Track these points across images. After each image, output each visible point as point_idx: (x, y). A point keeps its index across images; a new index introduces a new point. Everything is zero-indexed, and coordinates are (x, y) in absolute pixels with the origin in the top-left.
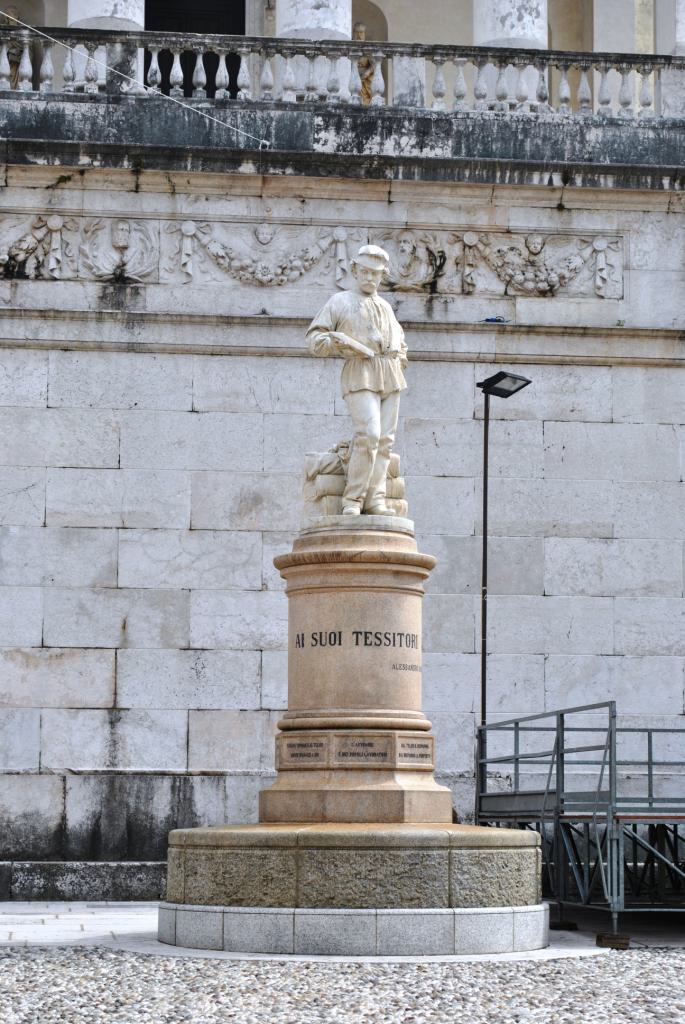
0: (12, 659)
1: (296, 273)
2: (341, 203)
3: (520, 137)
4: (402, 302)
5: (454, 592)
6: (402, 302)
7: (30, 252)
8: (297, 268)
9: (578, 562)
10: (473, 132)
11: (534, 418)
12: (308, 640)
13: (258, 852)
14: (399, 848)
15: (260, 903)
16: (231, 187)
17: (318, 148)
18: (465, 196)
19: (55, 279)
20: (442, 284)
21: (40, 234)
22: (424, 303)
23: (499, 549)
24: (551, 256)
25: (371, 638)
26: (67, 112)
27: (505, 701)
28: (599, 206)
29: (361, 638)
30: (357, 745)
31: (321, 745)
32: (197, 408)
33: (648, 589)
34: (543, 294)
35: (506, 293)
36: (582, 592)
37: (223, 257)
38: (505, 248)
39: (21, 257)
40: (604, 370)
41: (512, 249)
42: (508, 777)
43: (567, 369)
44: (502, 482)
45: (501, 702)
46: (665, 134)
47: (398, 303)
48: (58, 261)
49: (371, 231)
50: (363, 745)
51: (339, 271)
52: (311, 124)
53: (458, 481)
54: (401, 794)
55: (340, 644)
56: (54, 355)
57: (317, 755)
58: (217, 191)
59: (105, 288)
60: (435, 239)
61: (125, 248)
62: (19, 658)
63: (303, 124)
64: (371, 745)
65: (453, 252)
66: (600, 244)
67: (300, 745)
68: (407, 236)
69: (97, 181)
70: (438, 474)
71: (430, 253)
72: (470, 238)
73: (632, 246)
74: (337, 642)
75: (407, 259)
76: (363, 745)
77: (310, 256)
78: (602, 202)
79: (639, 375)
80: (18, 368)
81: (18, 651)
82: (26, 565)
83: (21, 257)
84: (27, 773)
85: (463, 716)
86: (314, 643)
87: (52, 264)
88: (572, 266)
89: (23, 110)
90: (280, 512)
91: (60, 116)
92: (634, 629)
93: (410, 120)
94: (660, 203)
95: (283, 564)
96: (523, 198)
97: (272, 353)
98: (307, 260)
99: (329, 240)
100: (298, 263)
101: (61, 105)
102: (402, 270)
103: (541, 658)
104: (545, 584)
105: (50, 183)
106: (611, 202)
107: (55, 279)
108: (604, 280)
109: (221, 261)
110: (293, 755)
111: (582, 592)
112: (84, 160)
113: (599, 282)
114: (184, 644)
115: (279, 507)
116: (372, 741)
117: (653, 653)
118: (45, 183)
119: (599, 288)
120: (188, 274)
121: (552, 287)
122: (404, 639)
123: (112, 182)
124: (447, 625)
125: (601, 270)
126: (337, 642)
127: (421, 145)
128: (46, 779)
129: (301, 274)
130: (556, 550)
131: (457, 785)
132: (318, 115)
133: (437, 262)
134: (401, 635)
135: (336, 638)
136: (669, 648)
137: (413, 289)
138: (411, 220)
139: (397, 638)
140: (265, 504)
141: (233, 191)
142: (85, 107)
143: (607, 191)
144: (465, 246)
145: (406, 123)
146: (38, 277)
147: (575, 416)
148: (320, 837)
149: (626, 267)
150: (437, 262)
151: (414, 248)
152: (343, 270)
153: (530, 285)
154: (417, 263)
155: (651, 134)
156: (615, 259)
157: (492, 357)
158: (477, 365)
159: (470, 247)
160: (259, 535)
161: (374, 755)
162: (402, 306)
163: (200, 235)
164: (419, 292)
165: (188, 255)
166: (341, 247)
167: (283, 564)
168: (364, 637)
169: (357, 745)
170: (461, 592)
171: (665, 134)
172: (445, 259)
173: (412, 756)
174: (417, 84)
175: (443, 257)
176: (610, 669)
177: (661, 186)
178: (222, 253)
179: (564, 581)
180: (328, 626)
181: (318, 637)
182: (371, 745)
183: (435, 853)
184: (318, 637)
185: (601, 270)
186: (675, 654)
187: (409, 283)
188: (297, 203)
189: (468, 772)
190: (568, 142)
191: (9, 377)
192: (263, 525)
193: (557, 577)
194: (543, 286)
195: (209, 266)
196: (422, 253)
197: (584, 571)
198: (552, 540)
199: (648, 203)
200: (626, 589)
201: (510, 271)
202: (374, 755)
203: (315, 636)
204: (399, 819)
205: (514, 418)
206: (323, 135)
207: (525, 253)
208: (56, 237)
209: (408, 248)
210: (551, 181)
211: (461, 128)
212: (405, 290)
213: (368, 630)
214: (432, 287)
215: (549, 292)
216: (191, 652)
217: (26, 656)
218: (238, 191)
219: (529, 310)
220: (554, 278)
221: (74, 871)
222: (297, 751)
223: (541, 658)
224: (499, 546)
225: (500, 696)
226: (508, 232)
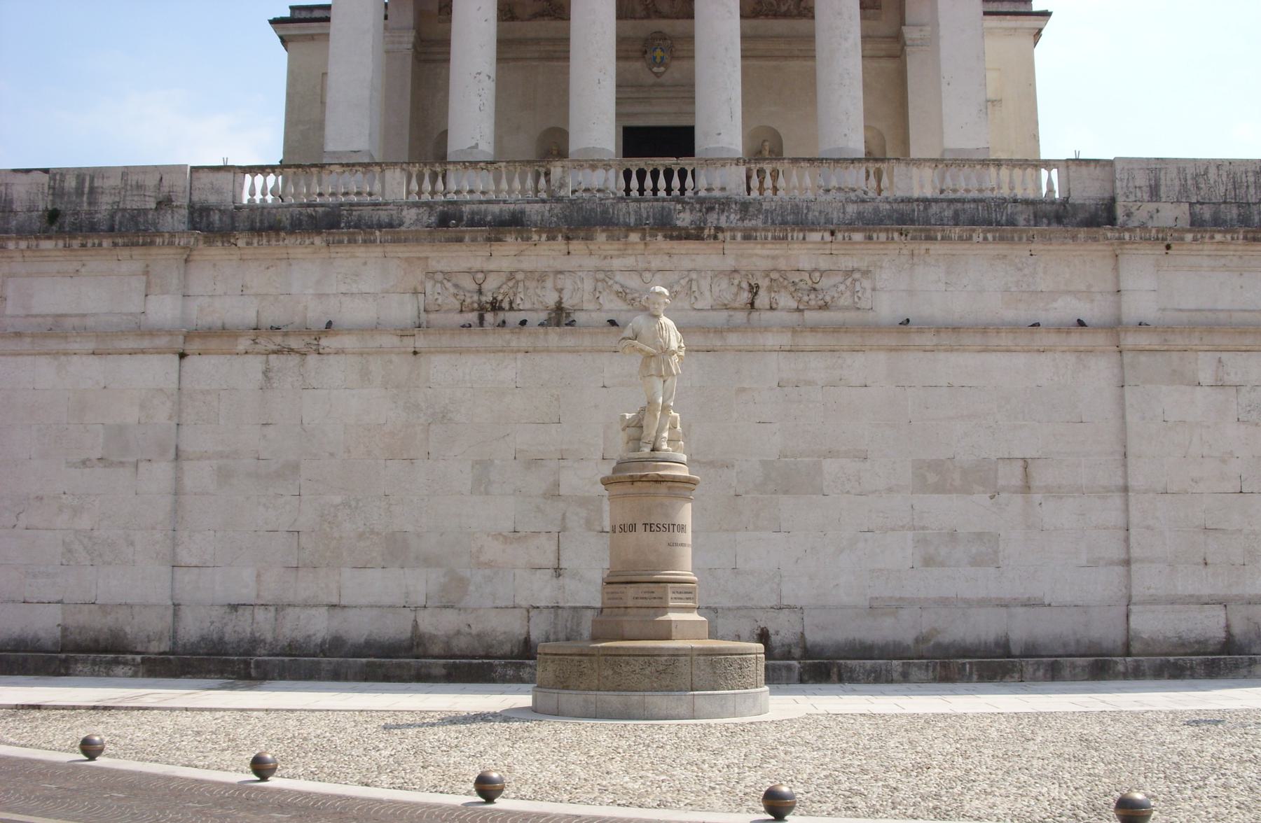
0: (497, 540)
2: (694, 257)
3: (805, 211)
7: (505, 294)
10: (775, 210)
11: (817, 385)
12: (618, 529)
13: (577, 658)
14: (659, 655)
15: (578, 688)
16: (625, 250)
17: (679, 223)
18: (771, 249)
19: (521, 310)
21: (511, 284)
24: (825, 283)
25: (654, 527)
26: (526, 210)
28: (855, 252)
29: (648, 527)
30: (645, 592)
32: (606, 384)
33: (890, 490)
34: (820, 308)
36: (848, 492)
38: (797, 280)
39: (500, 298)
40: (860, 354)
41: (801, 281)
43: (837, 354)
45: (797, 562)
46: (895, 206)
47: (730, 316)
48: (522, 299)
50: (649, 592)
52: (675, 209)
53: (768, 425)
54: (670, 622)
56: (520, 355)
58: (616, 253)
59: (549, 314)
61: (562, 289)
62: (501, 539)
63: (670, 209)
64: (653, 592)
65: (764, 283)
66: (857, 275)
69: (544, 250)
71: (750, 285)
72: (774, 275)
73: (877, 277)
75: (734, 289)
76: (649, 592)
78: (857, 249)
79: (882, 356)
80: (498, 365)
81: (500, 534)
82: (504, 482)
83: (500, 298)
84: (507, 608)
87: (518, 301)
88: (839, 290)
89: (501, 211)
91: (523, 212)
92: (881, 515)
93: (736, 203)
94: (895, 249)
95: (606, 482)
96: (808, 249)
99: (687, 279)
101: (523, 206)
102: (732, 296)
105: (516, 253)
106: (863, 249)
107: (521, 310)
108: (859, 298)
109: (620, 295)
111: (848, 492)
112: (535, 237)
113: (856, 300)
114: (599, 529)
117: (893, 530)
118: (513, 253)
119: (857, 303)
120: (600, 304)
121: (826, 303)
122: (676, 528)
123: (553, 250)
125: (858, 292)
127: (742, 219)
128: (517, 611)
130: (830, 466)
133: (754, 290)
134: (674, 525)
135: (633, 527)
136: (903, 527)
139: (671, 527)
141: (627, 252)
142: (537, 206)
143: (860, 243)
144: (772, 279)
145: (734, 206)
146: (511, 309)
148: (655, 649)
149: (874, 289)
150: (754, 290)
152: (695, 297)
153: (813, 303)
154: (742, 291)
155: (888, 207)
156: (867, 284)
157: (788, 348)
163: (607, 279)
165: (600, 292)
166: (694, 283)
167: (606, 482)
168: (649, 526)
169: (645, 592)
171: (895, 206)
173: (681, 599)
175: (758, 287)
176: (866, 540)
177: (893, 239)
178: (621, 290)
180: (629, 521)
181: (622, 527)
182: (653, 592)
183: (682, 658)
184: (622, 527)
185: (858, 292)
187: (737, 305)
188: (667, 258)
190: (835, 213)
191: (493, 370)
194: (821, 303)
195: (613, 297)
196: (745, 285)
197: (849, 480)
198: (829, 460)
199: (886, 249)
200: (876, 491)
201: (800, 295)
204: (668, 638)
206: (682, 215)
207: (810, 282)
208: (521, 285)
209: (736, 282)
211: (768, 208)
212: (735, 309)
215: (825, 307)
216: (604, 534)
217: (505, 537)
218: (630, 252)
219: (811, 316)
220: (828, 299)
221: (530, 666)
222: (611, 596)
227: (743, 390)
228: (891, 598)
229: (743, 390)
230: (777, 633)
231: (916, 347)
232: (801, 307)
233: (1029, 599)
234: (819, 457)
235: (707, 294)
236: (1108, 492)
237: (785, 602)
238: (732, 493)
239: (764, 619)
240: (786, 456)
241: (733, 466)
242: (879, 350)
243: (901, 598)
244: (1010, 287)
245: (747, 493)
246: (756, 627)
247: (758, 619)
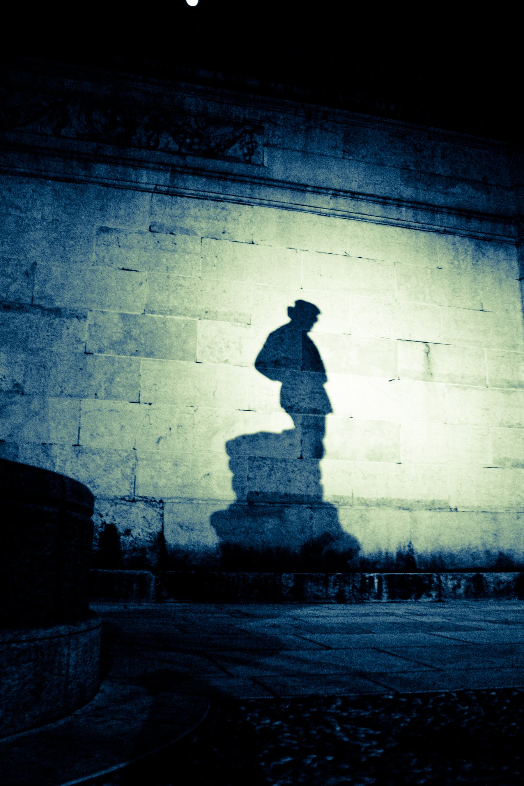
5: (125, 354)
9: (224, 339)
11: (196, 234)
23: (163, 325)
27: (161, 442)
42: (161, 501)
43: (221, 204)
45: (158, 442)
85: (126, 451)
104: (197, 355)
111: (226, 361)
124: (118, 379)
147: (226, 236)
158: (155, 195)
170: (131, 355)
179: (212, 353)
186: (296, 412)
189: (128, 496)
193: (207, 349)
197: (228, 347)
224: (164, 323)
225: (157, 437)
227: (106, 230)
228: (276, 493)
229: (107, 230)
230: (128, 532)
231: (312, 209)
232: (184, 151)
233: (433, 502)
234: (193, 316)
236: (513, 386)
237: (140, 492)
238: (81, 349)
239: (110, 513)
240: (153, 312)
241: (85, 317)
242: (270, 206)
243: (286, 495)
244: (408, 166)
245: (100, 351)
247: (103, 513)
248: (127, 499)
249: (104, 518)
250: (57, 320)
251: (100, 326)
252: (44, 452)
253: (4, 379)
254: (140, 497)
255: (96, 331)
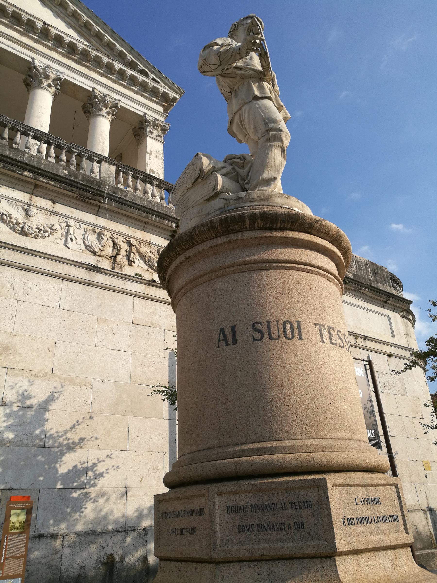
1: (47, 234)
4: (100, 261)
6: (100, 261)
8: (47, 231)
20: (119, 258)
22: (111, 264)
23: (142, 392)
31: (308, 504)
35: (148, 270)
37: (6, 215)
38: (148, 251)
42: (144, 529)
44: (145, 357)
45: (141, 480)
47: (98, 261)
49: (86, 226)
51: (69, 239)
55: (301, 338)
57: (300, 526)
60: (117, 238)
64: (376, 501)
67: (255, 508)
68: (105, 232)
70: (113, 348)
72: (133, 242)
74: (297, 335)
77: (54, 228)
86: (258, 336)
90: (20, 358)
93: (109, 186)
97: (27, 269)
98: (53, 230)
100: (48, 229)
103: (162, 454)
110: (241, 529)
115: (20, 355)
116: (377, 495)
126: (297, 335)
129: (48, 236)
131: (116, 537)
132: (66, 170)
137: (105, 257)
138: (106, 226)
140: (11, 352)
145: (107, 187)
151: (107, 239)
159: (133, 245)
160: (5, 370)
161: (384, 519)
162: (99, 263)
164: (107, 258)
172: (121, 249)
174: (112, 175)
182: (376, 501)
192: (7, 364)
202: (384, 519)
203: (258, 327)
205: (151, 326)
210: (172, 225)
213: (331, 325)
214: (114, 258)
223: (162, 454)
226: (149, 244)
227: (104, 321)
229: (104, 321)
235: (80, 241)
239: (111, 544)
245: (101, 411)
246: (102, 555)
248: (120, 530)
249: (105, 550)
250: (71, 387)
251: (101, 392)
252: (59, 496)
253: (29, 435)
254: (130, 527)
255: (98, 396)
